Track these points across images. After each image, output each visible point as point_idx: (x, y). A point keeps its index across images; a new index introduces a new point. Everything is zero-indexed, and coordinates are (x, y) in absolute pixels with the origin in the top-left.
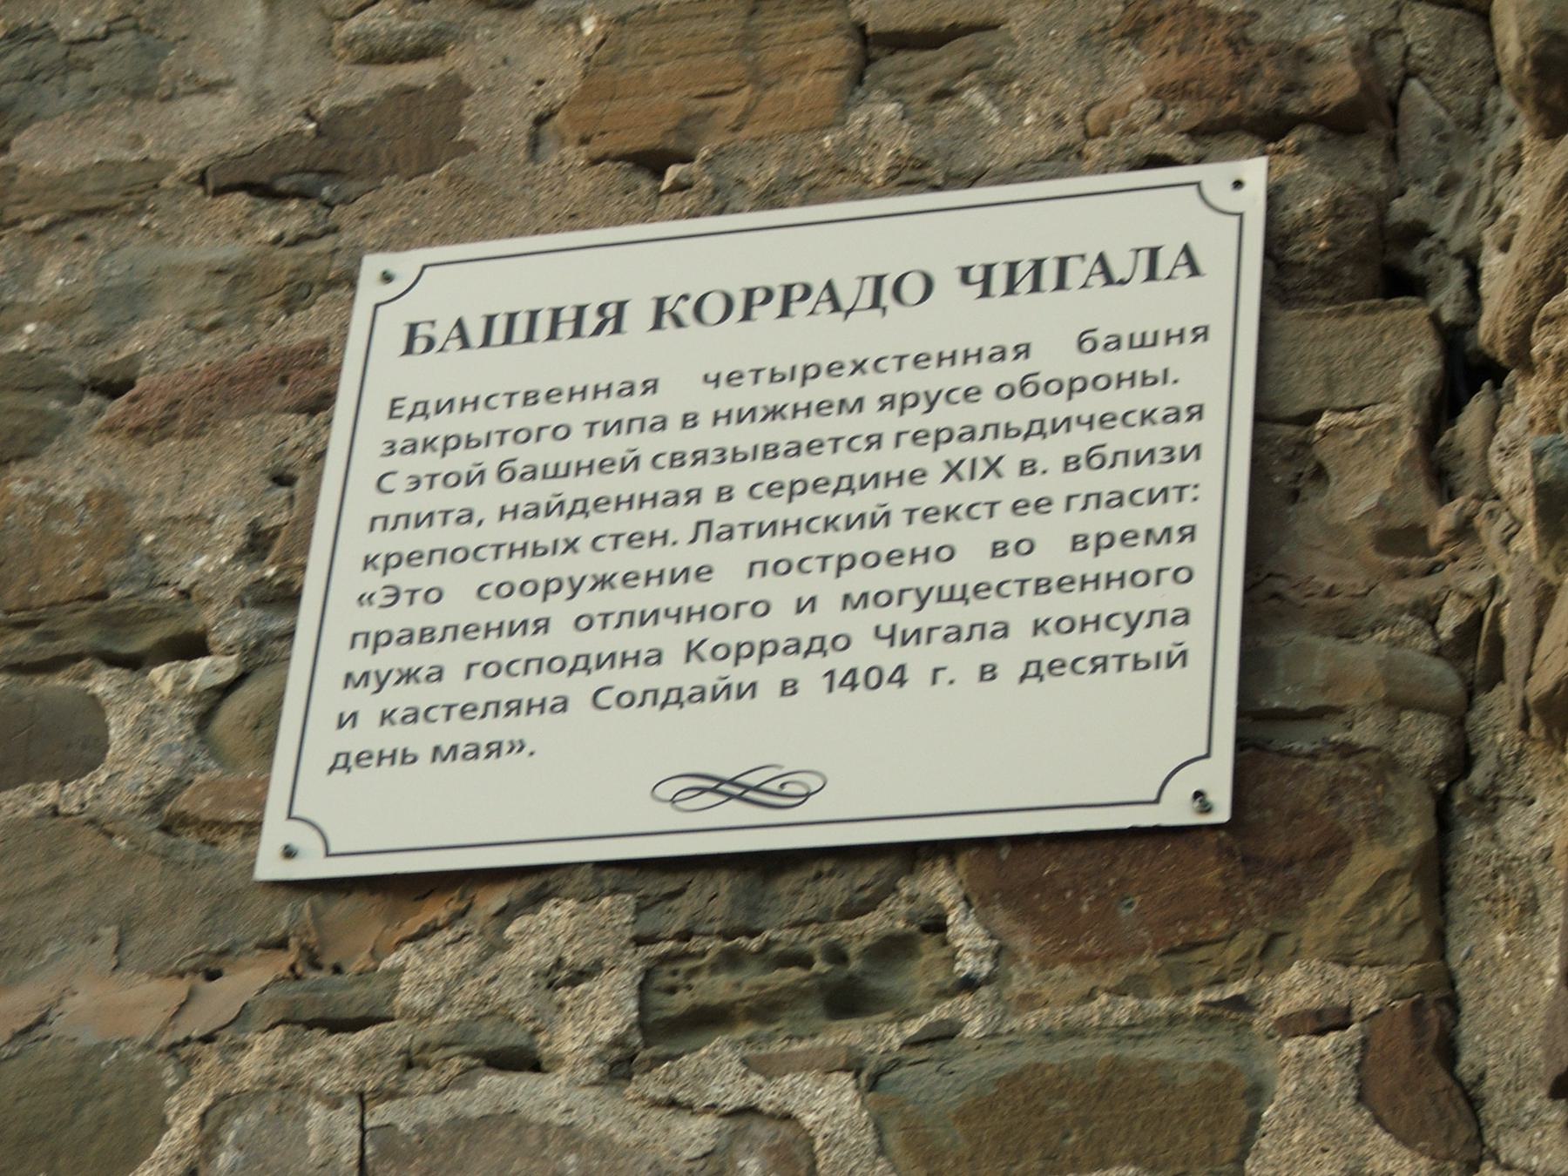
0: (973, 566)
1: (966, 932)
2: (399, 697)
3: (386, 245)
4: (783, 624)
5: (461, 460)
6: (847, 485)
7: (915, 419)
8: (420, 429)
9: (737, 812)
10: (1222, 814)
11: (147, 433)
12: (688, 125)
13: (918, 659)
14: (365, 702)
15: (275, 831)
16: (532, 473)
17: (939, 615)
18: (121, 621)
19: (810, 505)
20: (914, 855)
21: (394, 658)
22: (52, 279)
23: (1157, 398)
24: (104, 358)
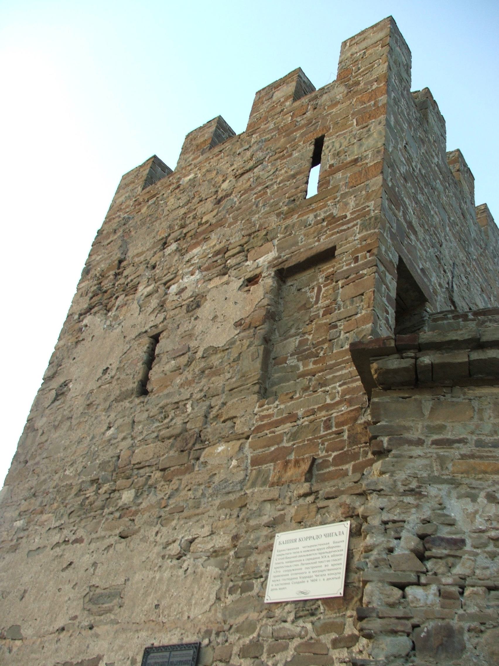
0: (323, 568)
1: (322, 607)
2: (277, 583)
3: (279, 533)
6: (314, 559)
7: (320, 551)
9: (303, 595)
10: (342, 595)
11: (259, 554)
12: (303, 518)
13: (318, 578)
14: (274, 583)
15: (266, 597)
17: (321, 573)
18: (255, 574)
20: (317, 600)
22: (252, 537)
23: (339, 549)
24: (256, 545)
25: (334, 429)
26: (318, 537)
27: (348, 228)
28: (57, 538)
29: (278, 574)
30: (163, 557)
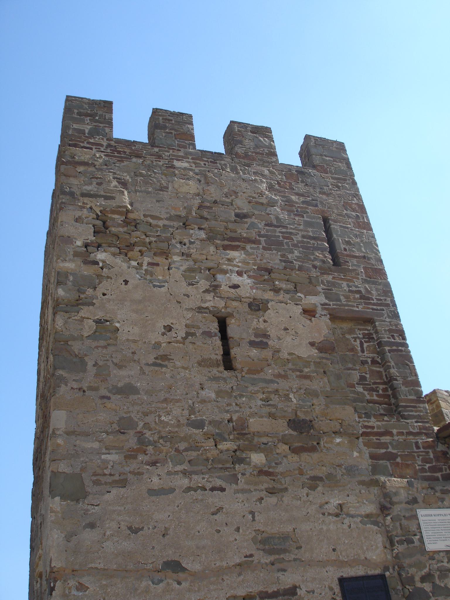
4: (447, 536)
5: (427, 524)
8: (425, 522)
16: (431, 525)
19: (446, 529)
21: (428, 537)
25: (422, 450)
26: (445, 515)
27: (377, 310)
28: (185, 482)
29: (428, 534)
30: (324, 514)
